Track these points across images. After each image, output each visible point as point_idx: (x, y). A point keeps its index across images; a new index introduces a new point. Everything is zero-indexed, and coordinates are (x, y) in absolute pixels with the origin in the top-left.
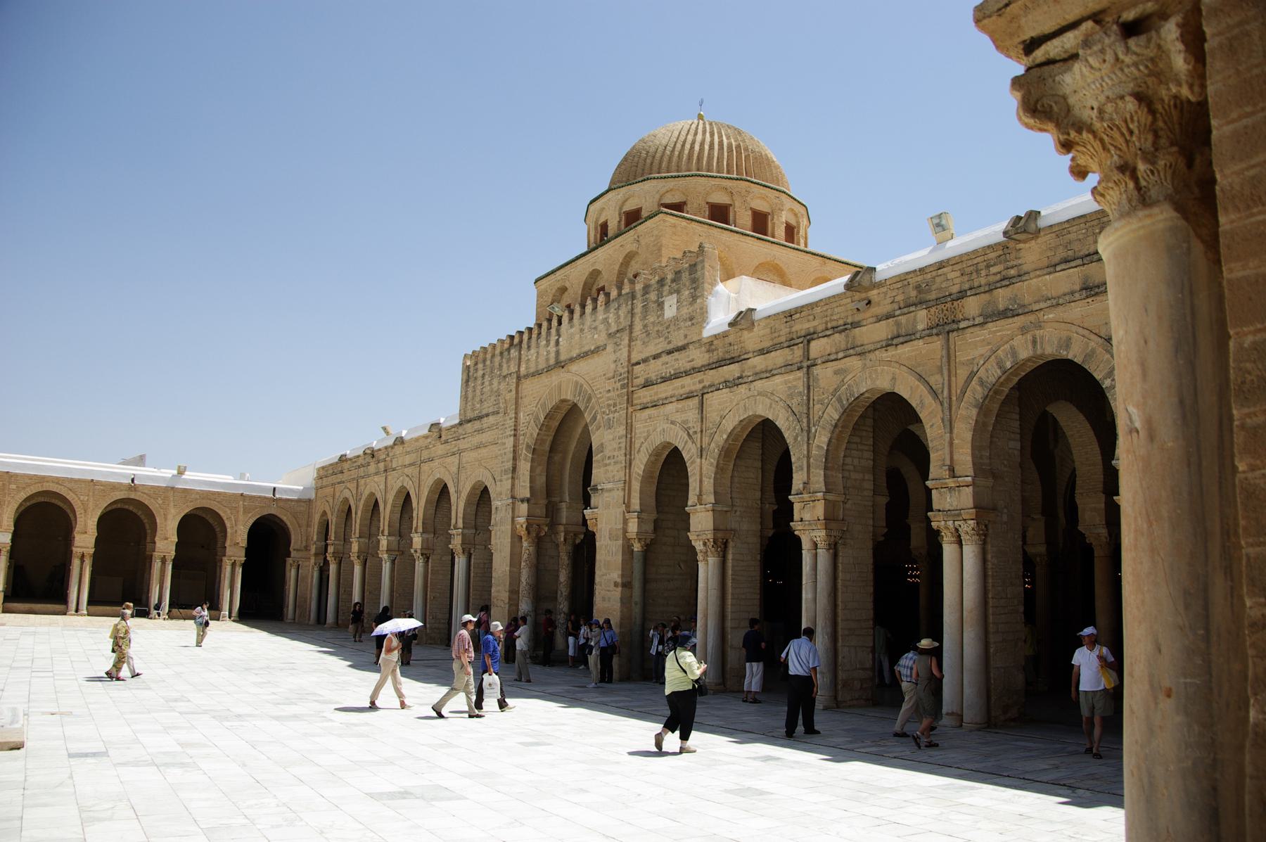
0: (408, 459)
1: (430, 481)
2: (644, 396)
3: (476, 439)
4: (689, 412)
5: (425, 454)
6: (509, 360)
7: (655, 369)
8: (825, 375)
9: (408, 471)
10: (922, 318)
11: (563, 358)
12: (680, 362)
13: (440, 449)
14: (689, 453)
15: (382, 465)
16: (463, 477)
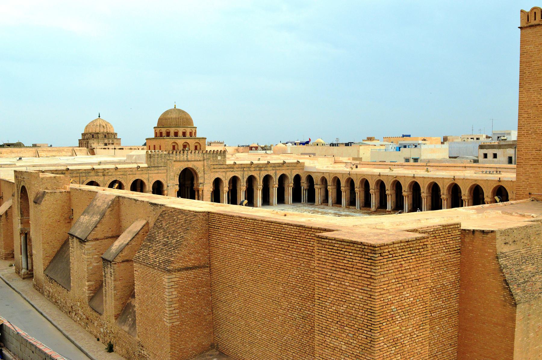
0: (119, 173)
1: (134, 179)
2: (214, 170)
3: (156, 171)
4: (224, 174)
5: (131, 173)
6: (169, 157)
7: (215, 166)
8: (246, 172)
9: (121, 176)
10: (258, 169)
11: (189, 159)
12: (222, 166)
13: (138, 172)
14: (223, 179)
15: (101, 174)
16: (150, 179)
